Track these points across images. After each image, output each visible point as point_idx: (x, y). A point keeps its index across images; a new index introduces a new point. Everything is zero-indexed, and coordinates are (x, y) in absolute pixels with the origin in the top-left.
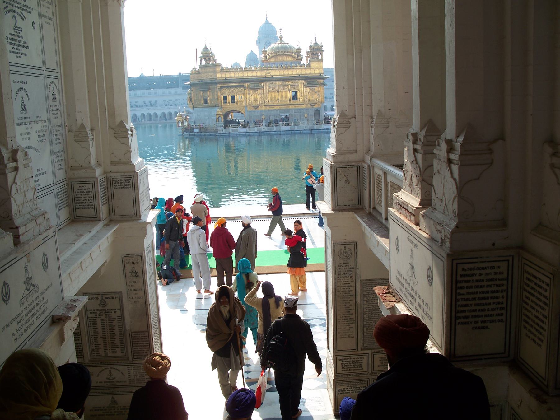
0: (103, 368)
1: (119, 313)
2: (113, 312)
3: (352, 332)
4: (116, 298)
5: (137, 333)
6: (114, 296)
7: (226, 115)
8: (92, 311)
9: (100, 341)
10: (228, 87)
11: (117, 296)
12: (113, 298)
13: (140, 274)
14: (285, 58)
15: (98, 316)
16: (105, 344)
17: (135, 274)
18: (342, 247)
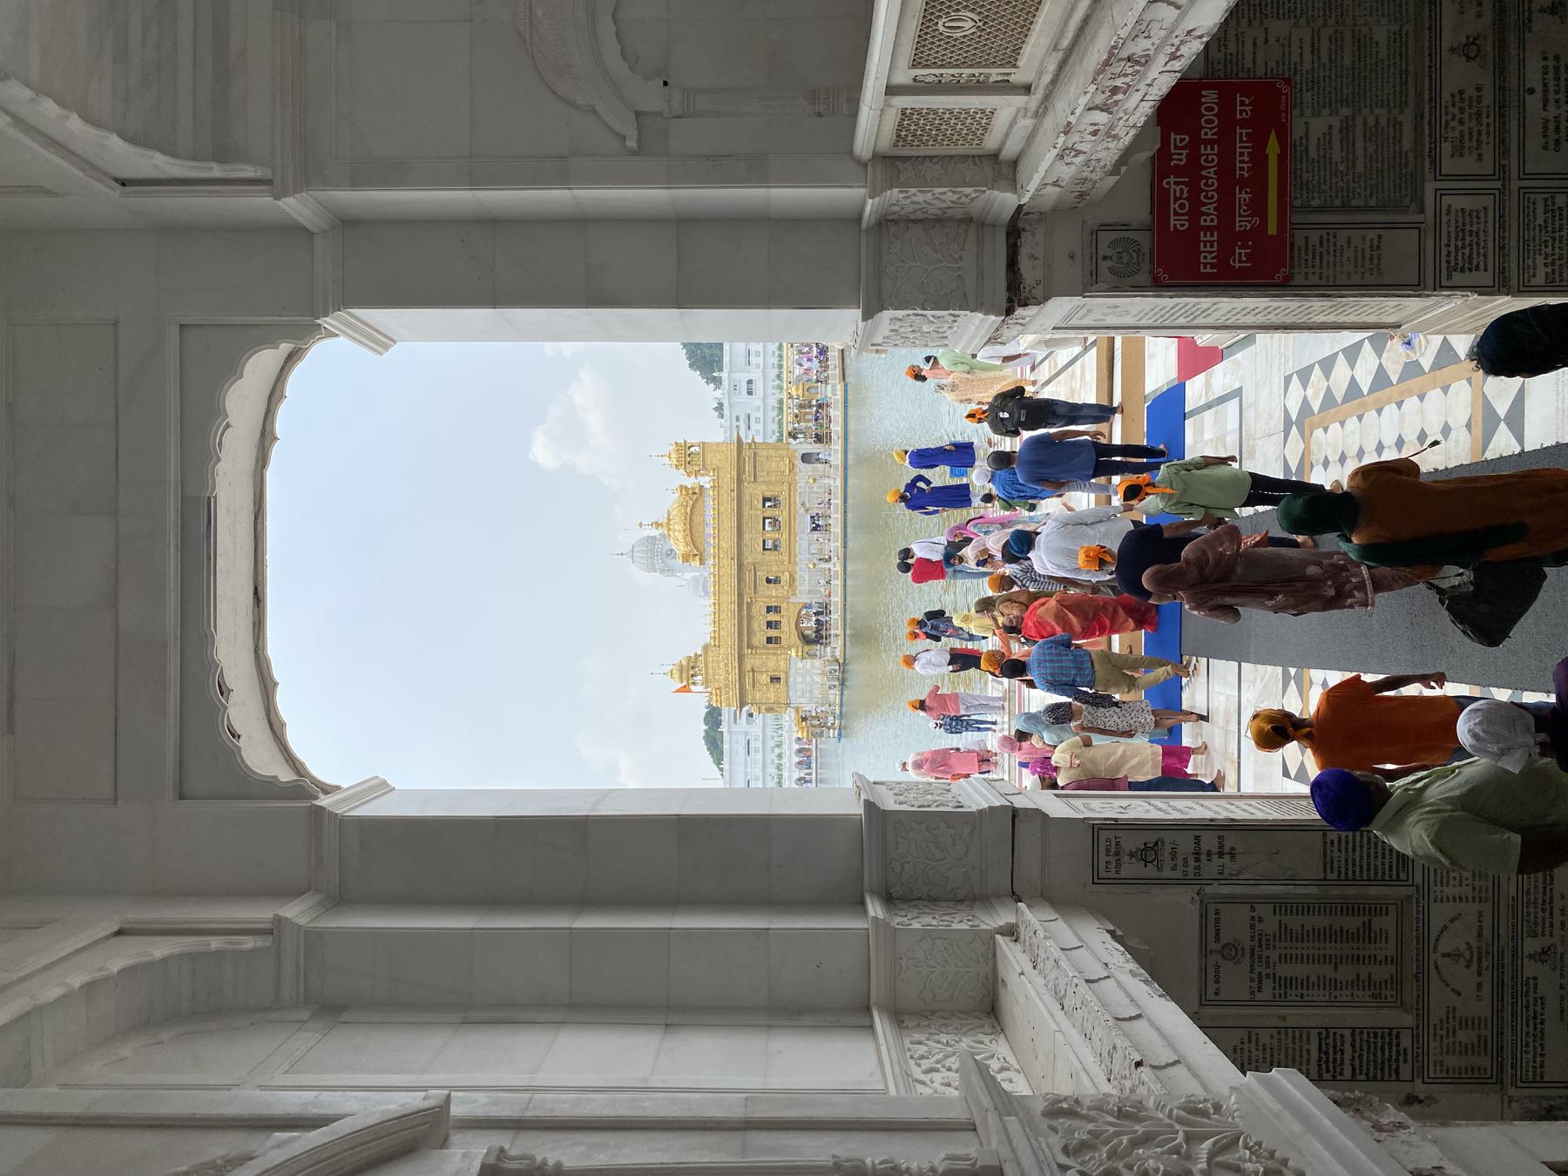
0: (1433, 973)
1: (1265, 911)
2: (1258, 926)
3: (1364, 238)
4: (1217, 912)
5: (1327, 864)
6: (1212, 917)
7: (806, 640)
8: (1255, 985)
9: (1346, 973)
11: (1212, 908)
12: (1217, 921)
13: (1151, 838)
14: (697, 519)
15: (1270, 971)
16: (1358, 959)
17: (1149, 853)
18: (1104, 266)
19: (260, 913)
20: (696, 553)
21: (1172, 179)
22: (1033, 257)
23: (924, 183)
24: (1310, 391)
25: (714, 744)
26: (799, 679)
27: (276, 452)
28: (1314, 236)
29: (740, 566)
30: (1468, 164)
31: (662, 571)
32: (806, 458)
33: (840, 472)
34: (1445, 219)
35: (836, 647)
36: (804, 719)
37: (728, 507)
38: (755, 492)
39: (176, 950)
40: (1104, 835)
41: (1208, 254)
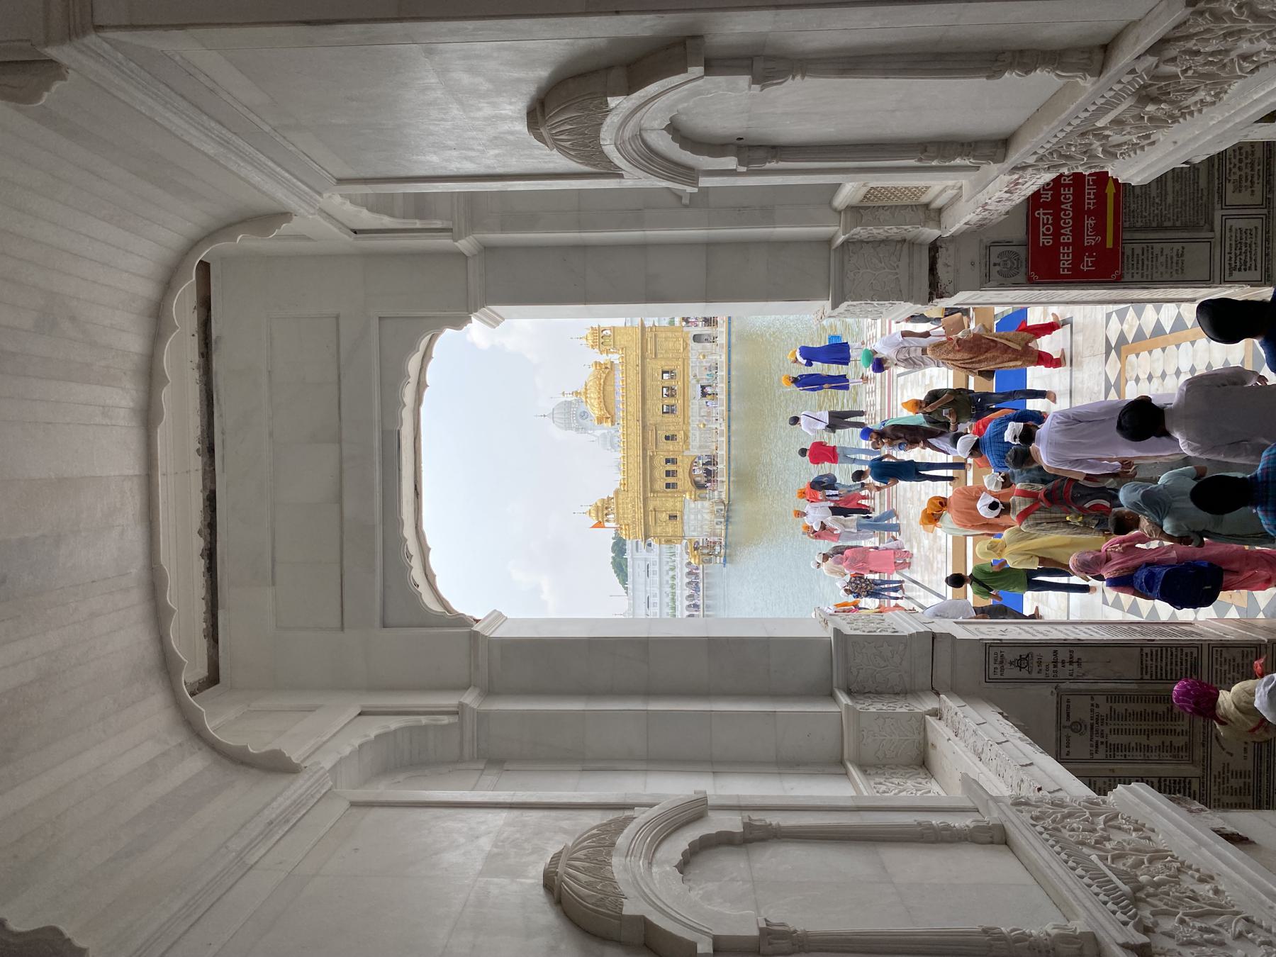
1: (1100, 700)
2: (1096, 710)
4: (1068, 701)
5: (1143, 668)
9: (1155, 741)
10: (652, 480)
11: (1065, 698)
12: (1068, 707)
13: (1024, 652)
14: (609, 388)
17: (1022, 662)
18: (994, 270)
19: (448, 701)
20: (608, 416)
21: (1041, 211)
22: (946, 265)
23: (878, 223)
24: (1126, 327)
25: (620, 568)
26: (692, 517)
27: (427, 395)
28: (1138, 249)
29: (644, 427)
30: (1245, 198)
31: (577, 429)
32: (697, 338)
33: (725, 350)
34: (1228, 234)
35: (721, 490)
36: (696, 549)
37: (635, 379)
38: (655, 366)
39: (403, 724)
40: (992, 651)
41: (1065, 263)
